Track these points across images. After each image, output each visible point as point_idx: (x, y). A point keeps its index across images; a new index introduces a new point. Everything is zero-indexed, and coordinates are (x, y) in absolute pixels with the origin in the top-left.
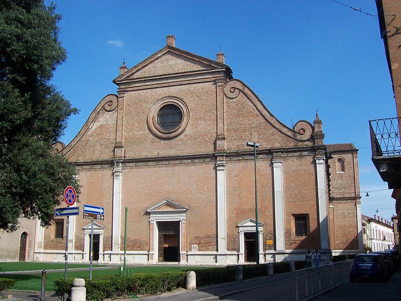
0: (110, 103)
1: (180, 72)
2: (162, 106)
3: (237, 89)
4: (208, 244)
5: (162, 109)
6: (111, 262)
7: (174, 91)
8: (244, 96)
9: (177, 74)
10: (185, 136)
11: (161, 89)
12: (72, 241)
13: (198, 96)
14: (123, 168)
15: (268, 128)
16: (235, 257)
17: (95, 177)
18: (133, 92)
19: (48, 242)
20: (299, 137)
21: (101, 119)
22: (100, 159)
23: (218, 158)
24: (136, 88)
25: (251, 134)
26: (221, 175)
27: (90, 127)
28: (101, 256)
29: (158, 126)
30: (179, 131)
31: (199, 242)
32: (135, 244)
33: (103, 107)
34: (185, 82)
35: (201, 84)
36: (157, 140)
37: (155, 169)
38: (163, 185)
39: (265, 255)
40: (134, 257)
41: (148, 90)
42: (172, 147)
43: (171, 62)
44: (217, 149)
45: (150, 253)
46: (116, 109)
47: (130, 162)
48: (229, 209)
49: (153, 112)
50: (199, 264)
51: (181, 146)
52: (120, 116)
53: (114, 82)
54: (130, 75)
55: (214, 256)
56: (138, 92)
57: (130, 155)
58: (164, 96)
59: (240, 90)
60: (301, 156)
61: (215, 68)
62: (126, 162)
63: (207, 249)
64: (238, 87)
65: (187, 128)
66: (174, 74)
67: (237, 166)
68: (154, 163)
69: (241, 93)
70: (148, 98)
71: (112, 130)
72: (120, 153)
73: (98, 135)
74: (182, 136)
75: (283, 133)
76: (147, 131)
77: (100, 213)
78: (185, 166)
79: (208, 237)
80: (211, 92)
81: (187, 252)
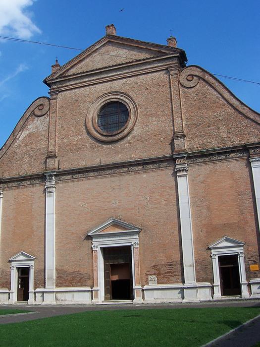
0: (41, 107)
2: (102, 104)
3: (195, 76)
5: (103, 108)
6: (44, 303)
7: (117, 85)
8: (205, 84)
9: (119, 65)
10: (134, 137)
11: (100, 85)
14: (57, 183)
16: (208, 291)
21: (30, 126)
22: (29, 174)
23: (178, 161)
24: (71, 87)
26: (183, 183)
27: (18, 137)
28: (31, 296)
29: (99, 129)
30: (126, 131)
32: (73, 278)
33: (33, 113)
35: (150, 74)
36: (99, 145)
37: (96, 181)
38: (108, 200)
39: (249, 285)
40: (73, 295)
41: (85, 88)
42: (117, 153)
44: (176, 149)
45: (94, 289)
46: (48, 113)
47: (65, 174)
48: (196, 226)
50: (159, 301)
51: (128, 149)
52: (53, 121)
53: (45, 82)
55: (179, 291)
56: (74, 91)
57: (65, 166)
58: (105, 92)
59: (199, 78)
62: (60, 174)
64: (197, 74)
65: (135, 128)
66: (116, 65)
67: (203, 170)
69: (201, 81)
71: (43, 138)
72: (53, 164)
74: (129, 138)
76: (85, 135)
78: (135, 174)
79: (169, 264)
81: (143, 286)
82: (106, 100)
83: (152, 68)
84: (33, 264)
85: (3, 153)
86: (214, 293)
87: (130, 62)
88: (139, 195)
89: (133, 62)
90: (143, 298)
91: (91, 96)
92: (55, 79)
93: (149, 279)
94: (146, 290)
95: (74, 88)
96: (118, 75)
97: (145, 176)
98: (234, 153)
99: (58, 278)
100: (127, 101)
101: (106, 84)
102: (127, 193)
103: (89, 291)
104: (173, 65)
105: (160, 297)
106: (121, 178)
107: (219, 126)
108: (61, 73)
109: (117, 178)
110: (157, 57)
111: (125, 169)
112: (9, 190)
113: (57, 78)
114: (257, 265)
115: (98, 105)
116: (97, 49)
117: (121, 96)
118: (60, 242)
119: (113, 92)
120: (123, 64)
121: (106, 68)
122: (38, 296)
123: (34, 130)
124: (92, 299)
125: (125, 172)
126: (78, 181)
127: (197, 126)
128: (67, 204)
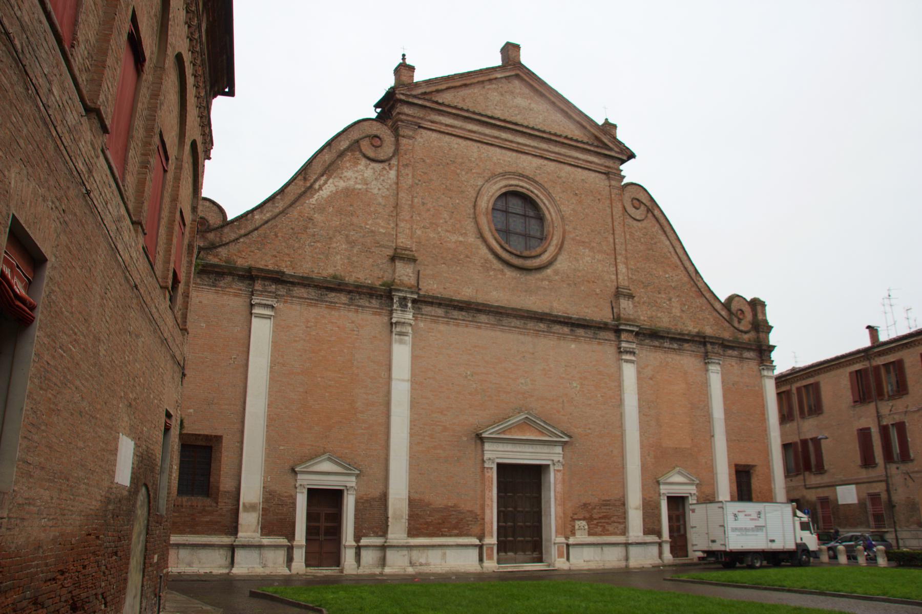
4: (607, 521)
5: (505, 195)
7: (528, 164)
9: (539, 130)
10: (556, 273)
11: (498, 150)
12: (251, 508)
13: (576, 194)
14: (415, 318)
18: (434, 135)
24: (443, 128)
25: (670, 300)
27: (317, 186)
31: (587, 515)
34: (552, 156)
35: (580, 170)
36: (497, 265)
40: (445, 554)
41: (469, 143)
47: (431, 304)
48: (642, 446)
52: (407, 181)
54: (431, 92)
56: (447, 138)
57: (430, 287)
61: (611, 149)
62: (421, 302)
63: (605, 532)
65: (560, 258)
67: (653, 357)
68: (492, 319)
72: (404, 273)
74: (549, 271)
76: (472, 239)
78: (559, 339)
80: (600, 194)
81: (567, 538)
85: (277, 211)
87: (555, 135)
89: (560, 136)
90: (568, 559)
92: (415, 97)
93: (577, 527)
97: (573, 346)
98: (688, 343)
99: (412, 517)
101: (509, 153)
103: (476, 546)
105: (592, 559)
108: (428, 90)
110: (587, 143)
111: (542, 325)
112: (292, 303)
113: (415, 97)
116: (496, 79)
117: (536, 188)
119: (523, 176)
120: (544, 132)
122: (368, 557)
123: (359, 186)
124: (481, 560)
126: (458, 325)
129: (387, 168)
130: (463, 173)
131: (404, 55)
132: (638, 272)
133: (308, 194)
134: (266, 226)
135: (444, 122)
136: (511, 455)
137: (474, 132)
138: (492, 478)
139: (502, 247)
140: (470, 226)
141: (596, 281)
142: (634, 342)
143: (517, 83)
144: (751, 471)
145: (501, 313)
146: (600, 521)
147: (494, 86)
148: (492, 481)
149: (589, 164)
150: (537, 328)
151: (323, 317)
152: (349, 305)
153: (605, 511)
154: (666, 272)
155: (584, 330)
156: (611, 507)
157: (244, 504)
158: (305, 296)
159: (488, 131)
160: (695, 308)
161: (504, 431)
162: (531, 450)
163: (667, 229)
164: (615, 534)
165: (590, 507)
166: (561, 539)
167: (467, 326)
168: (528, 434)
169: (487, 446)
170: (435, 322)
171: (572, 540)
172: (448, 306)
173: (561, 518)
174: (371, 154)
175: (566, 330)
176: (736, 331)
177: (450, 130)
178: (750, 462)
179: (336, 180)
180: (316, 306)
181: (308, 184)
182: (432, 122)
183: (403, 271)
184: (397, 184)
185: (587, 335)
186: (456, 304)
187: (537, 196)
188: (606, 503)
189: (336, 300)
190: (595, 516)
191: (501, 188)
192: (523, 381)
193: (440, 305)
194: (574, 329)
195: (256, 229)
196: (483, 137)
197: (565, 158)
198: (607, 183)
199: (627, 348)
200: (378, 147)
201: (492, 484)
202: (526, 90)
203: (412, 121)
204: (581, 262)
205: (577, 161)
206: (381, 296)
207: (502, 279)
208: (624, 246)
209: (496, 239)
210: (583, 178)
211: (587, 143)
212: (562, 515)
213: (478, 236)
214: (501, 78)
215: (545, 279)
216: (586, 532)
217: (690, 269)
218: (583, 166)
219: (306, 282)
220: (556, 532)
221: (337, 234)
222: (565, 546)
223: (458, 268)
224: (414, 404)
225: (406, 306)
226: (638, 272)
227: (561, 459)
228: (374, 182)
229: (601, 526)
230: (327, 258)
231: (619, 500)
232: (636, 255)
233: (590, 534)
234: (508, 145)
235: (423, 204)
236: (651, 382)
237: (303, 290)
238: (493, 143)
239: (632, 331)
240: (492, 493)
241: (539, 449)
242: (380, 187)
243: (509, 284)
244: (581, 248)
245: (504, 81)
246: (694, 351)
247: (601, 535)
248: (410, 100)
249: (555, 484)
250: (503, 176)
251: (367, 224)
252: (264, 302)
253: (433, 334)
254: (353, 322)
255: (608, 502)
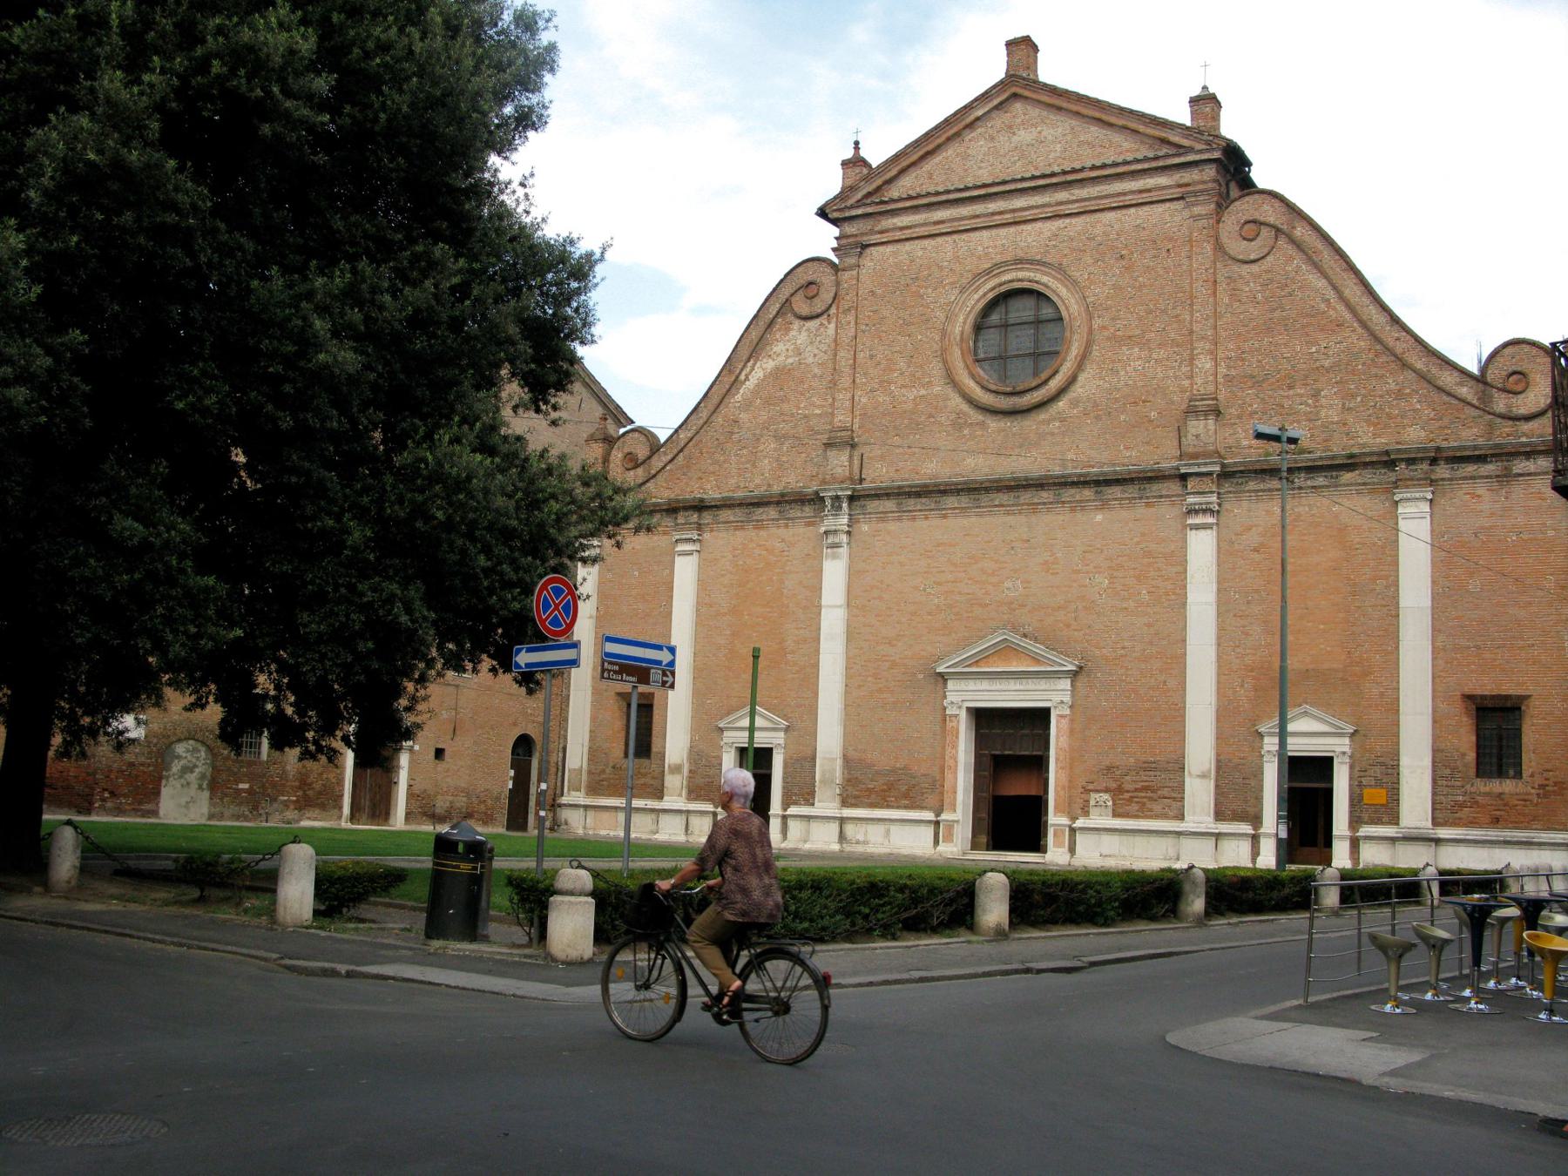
1: (1057, 169)
2: (991, 296)
4: (1150, 794)
6: (807, 846)
7: (1032, 238)
9: (1044, 176)
10: (1075, 403)
11: (985, 233)
12: (677, 769)
15: (1380, 372)
16: (1245, 847)
17: (757, 551)
18: (889, 249)
19: (603, 771)
20: (1501, 403)
21: (779, 347)
22: (776, 489)
23: (1190, 484)
24: (898, 235)
25: (1316, 395)
27: (742, 377)
30: (1054, 384)
32: (890, 787)
34: (1074, 208)
35: (1132, 210)
36: (977, 416)
37: (965, 522)
38: (994, 580)
40: (889, 830)
41: (940, 240)
43: (1024, 136)
45: (944, 817)
46: (833, 311)
49: (961, 319)
53: (822, 213)
54: (878, 189)
56: (908, 246)
57: (879, 473)
58: (998, 259)
59: (1278, 230)
60: (1506, 477)
61: (1190, 150)
64: (1271, 220)
65: (1082, 378)
66: (1034, 178)
68: (964, 500)
69: (1282, 242)
70: (941, 268)
73: (768, 402)
74: (1061, 404)
75: (1440, 389)
77: (659, 663)
78: (1073, 510)
80: (1170, 239)
81: (1074, 819)
82: (1001, 285)
83: (1141, 192)
84: (782, 742)
85: (701, 422)
86: (1258, 854)
87: (1074, 171)
88: (1078, 572)
89: (1082, 169)
90: (1072, 850)
91: (957, 267)
92: (852, 207)
93: (1092, 803)
94: (1081, 829)
95: (907, 240)
96: (1037, 207)
97: (1099, 517)
98: (1352, 471)
100: (1063, 291)
101: (1003, 232)
102: (1046, 562)
103: (930, 822)
104: (1201, 187)
106: (1034, 519)
107: (1319, 385)
109: (1022, 519)
110: (1156, 158)
111: (1044, 494)
112: (719, 531)
113: (859, 203)
114: (1384, 792)
115: (976, 296)
116: (978, 119)
117: (1045, 274)
118: (860, 686)
120: (1053, 175)
121: (1004, 182)
122: (795, 827)
123: (790, 360)
124: (936, 842)
125: (1044, 504)
126: (914, 519)
127: (1257, 382)
128: (882, 582)
129: (826, 323)
130: (930, 290)
131: (857, 143)
132: (1243, 360)
133: (733, 391)
134: (691, 444)
135: (900, 224)
136: (986, 696)
137: (942, 222)
138: (958, 729)
139: (983, 387)
140: (936, 369)
141: (1150, 398)
142: (1212, 492)
143: (1018, 106)
144: (1523, 708)
145: (975, 489)
146: (1136, 794)
147: (979, 130)
148: (958, 733)
149: (1144, 195)
150: (1036, 501)
151: (752, 540)
152: (778, 520)
153: (1145, 778)
154: (1310, 343)
155: (1121, 488)
156: (1159, 773)
157: (669, 766)
158: (732, 518)
159: (965, 211)
160: (1381, 396)
161: (977, 661)
162: (1018, 687)
163: (1326, 256)
164: (1165, 817)
165: (1117, 773)
166: (1064, 821)
167: (927, 518)
168: (1015, 663)
169: (951, 685)
170: (882, 520)
171: (1079, 823)
172: (899, 494)
173: (1063, 788)
174: (805, 311)
175: (1088, 493)
176: (1499, 420)
177: (907, 234)
178: (1509, 688)
179: (765, 360)
180: (742, 528)
181: (733, 378)
182: (881, 232)
183: (835, 462)
184: (835, 341)
185: (1127, 495)
186: (907, 490)
187: (1046, 286)
188: (1148, 767)
189: (764, 517)
190: (1127, 786)
191: (985, 295)
192: (1010, 585)
193: (888, 495)
194: (1100, 489)
195: (681, 451)
196: (956, 224)
197: (1099, 202)
198: (1186, 213)
199: (1195, 504)
200: (813, 297)
201: (957, 737)
202: (1034, 112)
203: (850, 244)
204: (1123, 373)
205: (1122, 198)
206: (813, 500)
207: (983, 436)
208: (1212, 321)
209: (973, 376)
210: (1138, 222)
211: (1146, 159)
212: (1067, 784)
213: (947, 381)
214: (989, 112)
215: (1054, 419)
216: (1110, 810)
217: (1378, 319)
218: (1134, 202)
219: (727, 504)
220: (1055, 808)
221: (765, 432)
222: (1067, 829)
223: (917, 437)
224: (851, 635)
225: (840, 508)
226: (1243, 360)
227: (1067, 699)
228: (809, 348)
229: (1137, 802)
230: (754, 466)
231: (1176, 762)
232: (1242, 330)
233: (1116, 815)
234: (998, 219)
235: (872, 357)
236: (1256, 556)
237: (729, 512)
238: (974, 226)
239: (1209, 474)
240: (957, 752)
241: (1031, 684)
242: (816, 351)
243: (993, 442)
244: (1124, 348)
245: (995, 114)
246: (1364, 484)
247: (1136, 817)
248: (847, 214)
249: (1057, 737)
250: (988, 274)
251: (799, 408)
252: (684, 537)
253: (880, 538)
254: (783, 541)
255: (1154, 765)
